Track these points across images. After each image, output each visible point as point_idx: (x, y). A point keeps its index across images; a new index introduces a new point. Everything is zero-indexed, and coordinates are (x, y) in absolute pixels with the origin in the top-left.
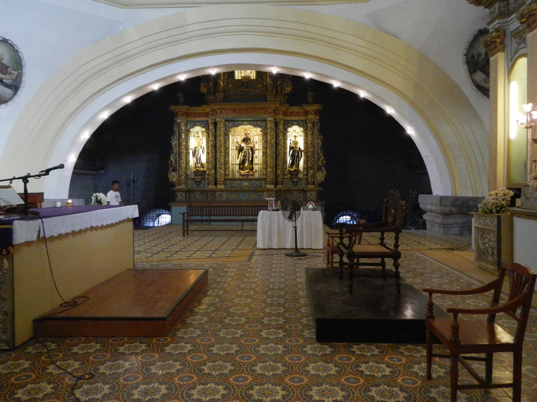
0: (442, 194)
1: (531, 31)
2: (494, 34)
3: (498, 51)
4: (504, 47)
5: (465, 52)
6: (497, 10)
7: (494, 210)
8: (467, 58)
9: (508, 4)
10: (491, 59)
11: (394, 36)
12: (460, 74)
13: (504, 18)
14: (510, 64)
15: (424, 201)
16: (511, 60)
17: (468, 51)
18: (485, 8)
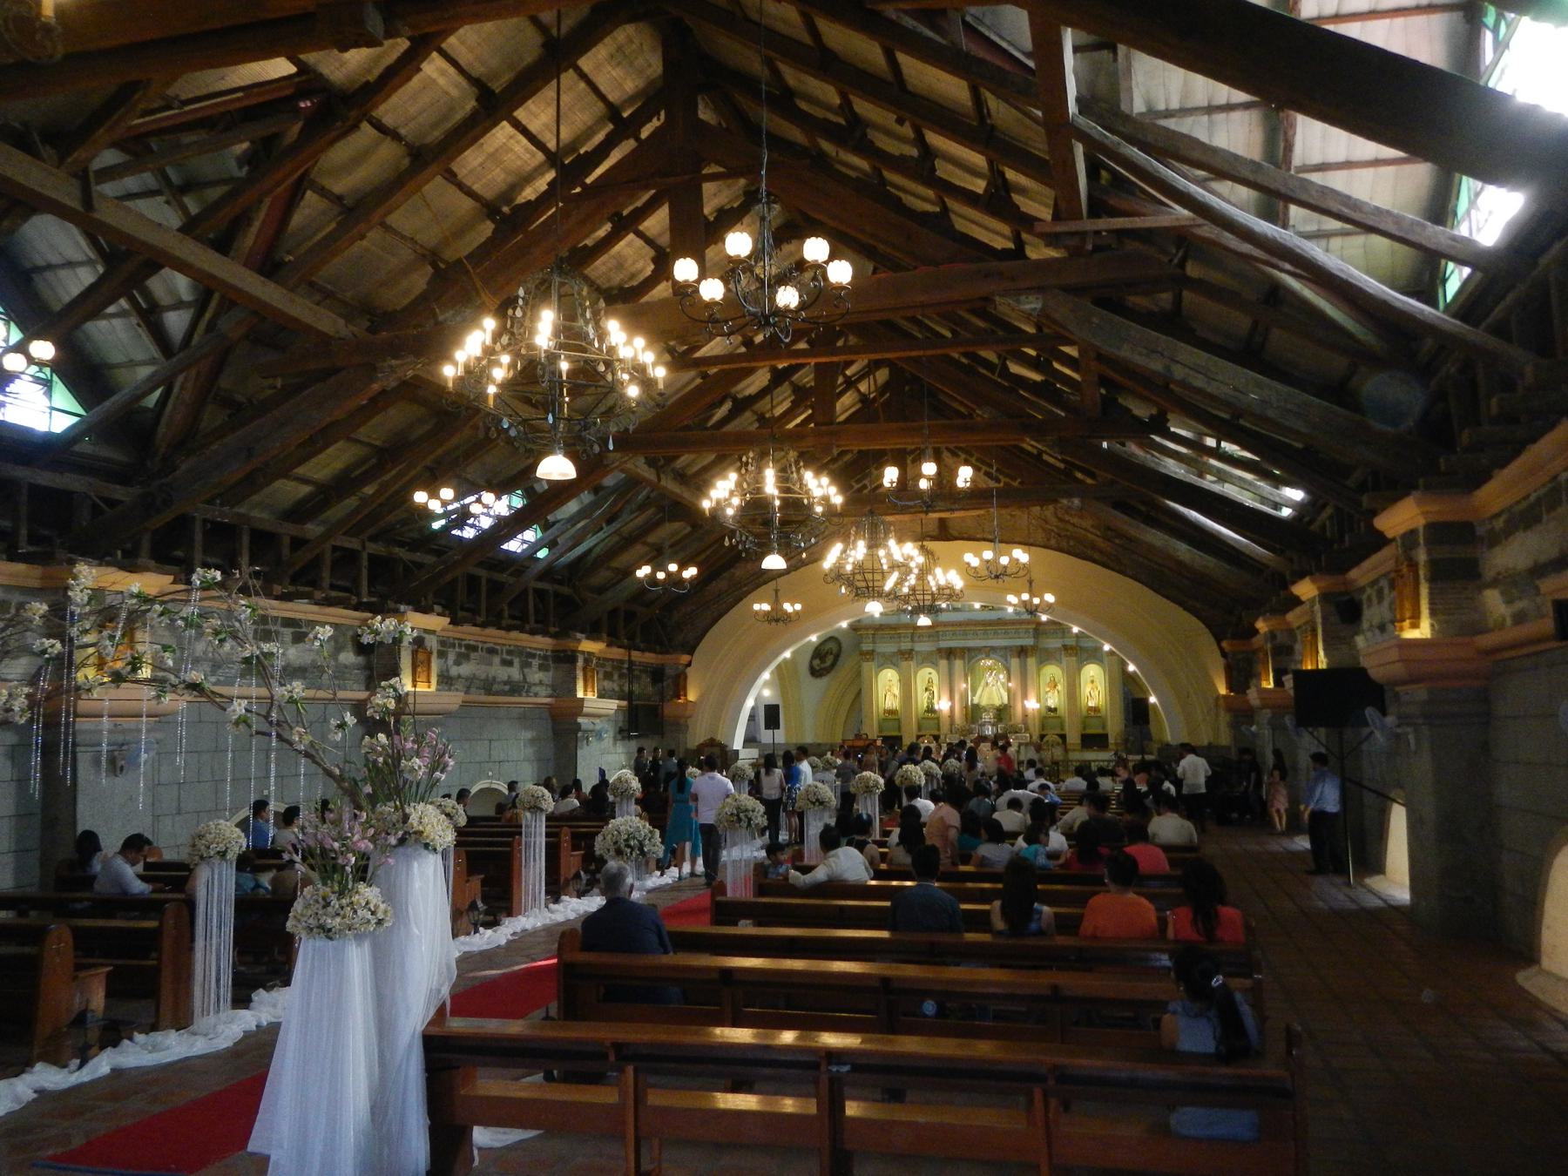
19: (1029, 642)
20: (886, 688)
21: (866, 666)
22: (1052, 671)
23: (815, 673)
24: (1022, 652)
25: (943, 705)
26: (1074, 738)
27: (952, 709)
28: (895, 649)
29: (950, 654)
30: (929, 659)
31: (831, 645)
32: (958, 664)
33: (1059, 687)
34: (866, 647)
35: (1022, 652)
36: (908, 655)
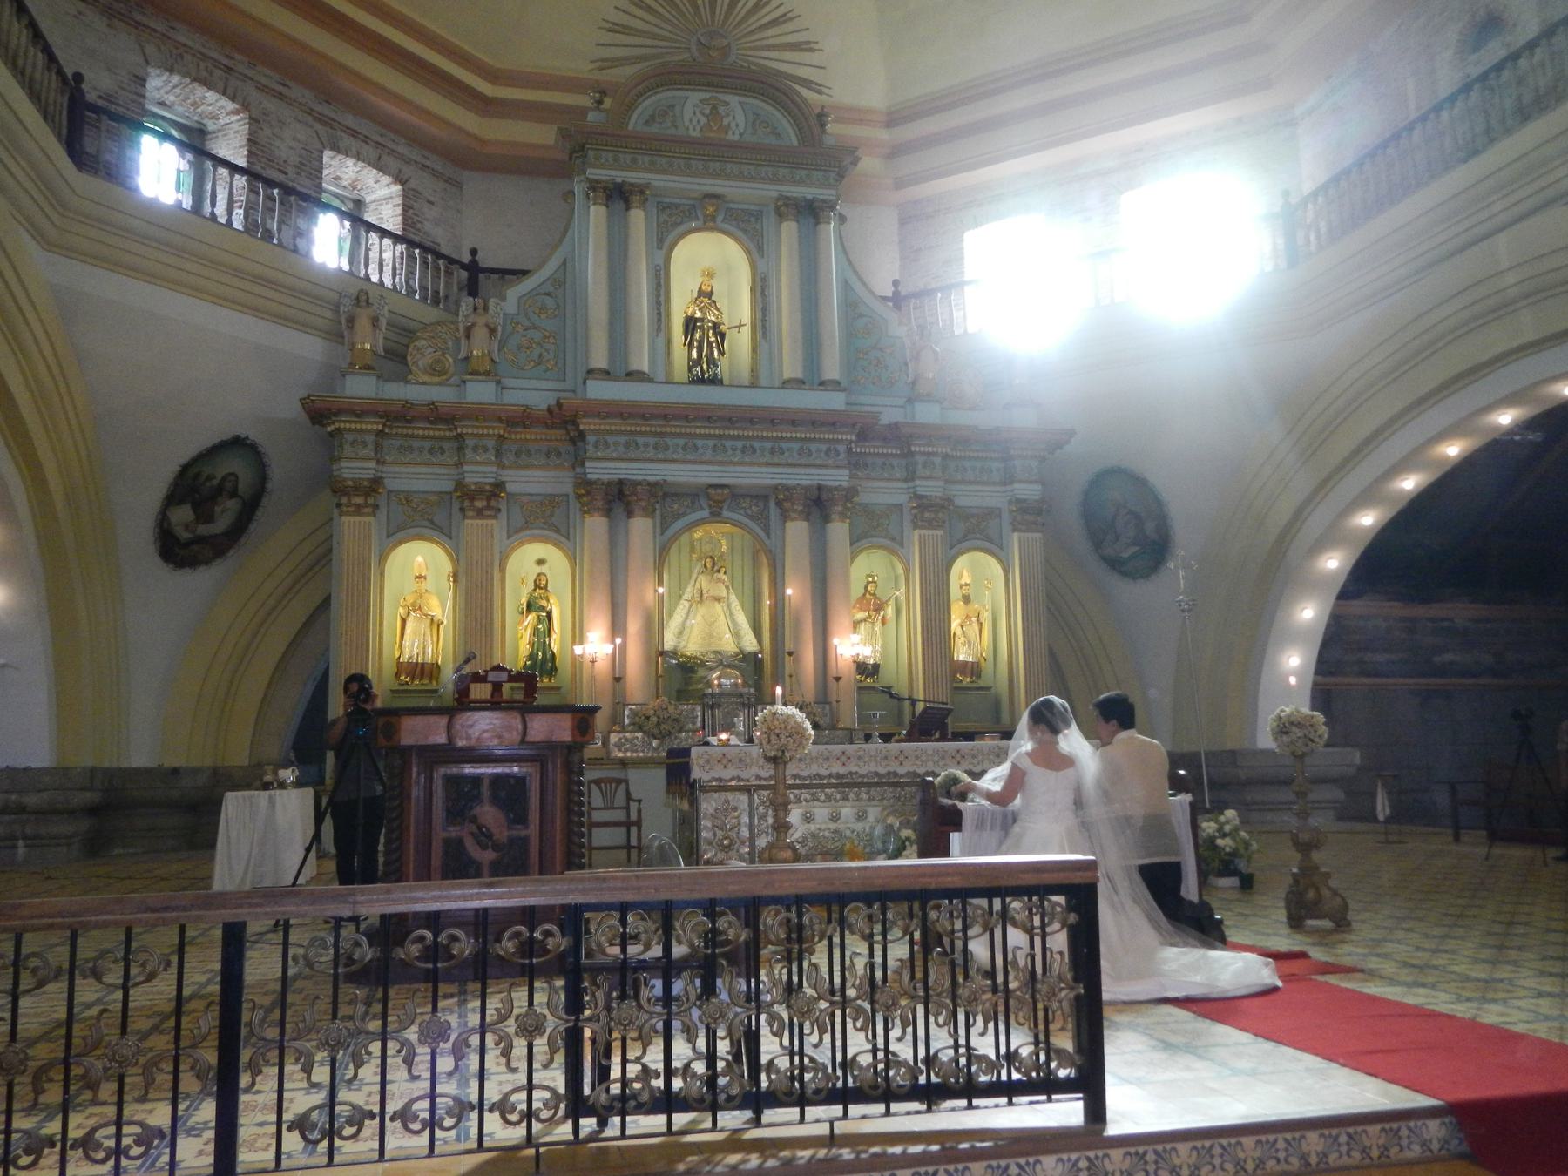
19: (836, 477)
20: (413, 604)
21: (350, 525)
22: (867, 568)
23: (176, 550)
24: (818, 505)
25: (596, 646)
27: (618, 659)
28: (448, 486)
29: (618, 499)
30: (547, 518)
31: (234, 465)
32: (641, 528)
33: (890, 611)
34: (354, 469)
35: (818, 505)
36: (483, 500)
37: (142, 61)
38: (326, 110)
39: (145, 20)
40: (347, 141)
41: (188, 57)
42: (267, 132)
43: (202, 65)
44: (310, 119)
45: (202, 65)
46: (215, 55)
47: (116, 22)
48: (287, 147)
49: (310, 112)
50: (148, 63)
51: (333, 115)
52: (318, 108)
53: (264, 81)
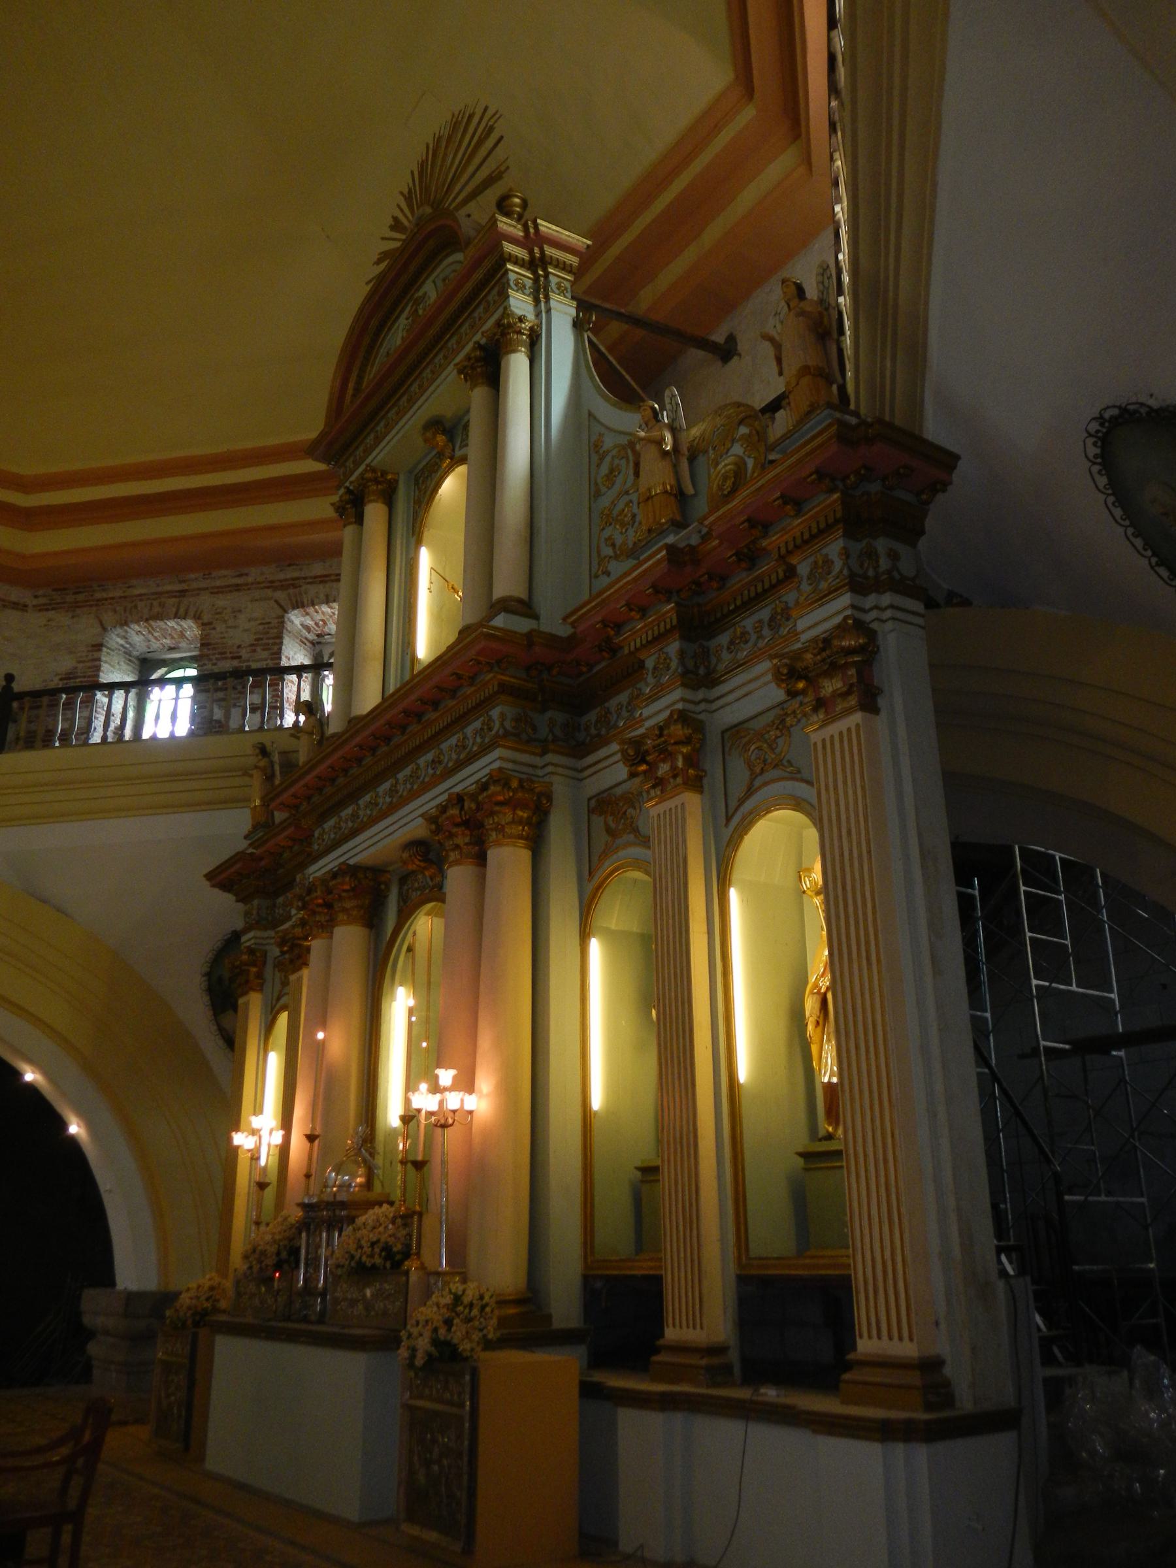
0: (133, 1286)
1: (294, 972)
2: (245, 957)
3: (254, 990)
4: (262, 985)
5: (206, 969)
6: (255, 912)
7: (189, 1322)
8: (209, 980)
9: (274, 905)
10: (241, 1001)
11: (59, 910)
12: (194, 1010)
13: (266, 929)
14: (270, 1017)
15: (96, 1308)
16: (272, 1009)
17: (211, 967)
18: (237, 901)
26: (703, 1313)
37: (100, 629)
38: (292, 573)
39: (105, 595)
40: (313, 590)
41: (140, 605)
42: (220, 627)
43: (155, 603)
44: (269, 592)
45: (155, 603)
46: (169, 588)
47: (78, 611)
48: (240, 634)
49: (272, 585)
50: (105, 629)
51: (296, 574)
52: (281, 576)
53: (218, 583)
